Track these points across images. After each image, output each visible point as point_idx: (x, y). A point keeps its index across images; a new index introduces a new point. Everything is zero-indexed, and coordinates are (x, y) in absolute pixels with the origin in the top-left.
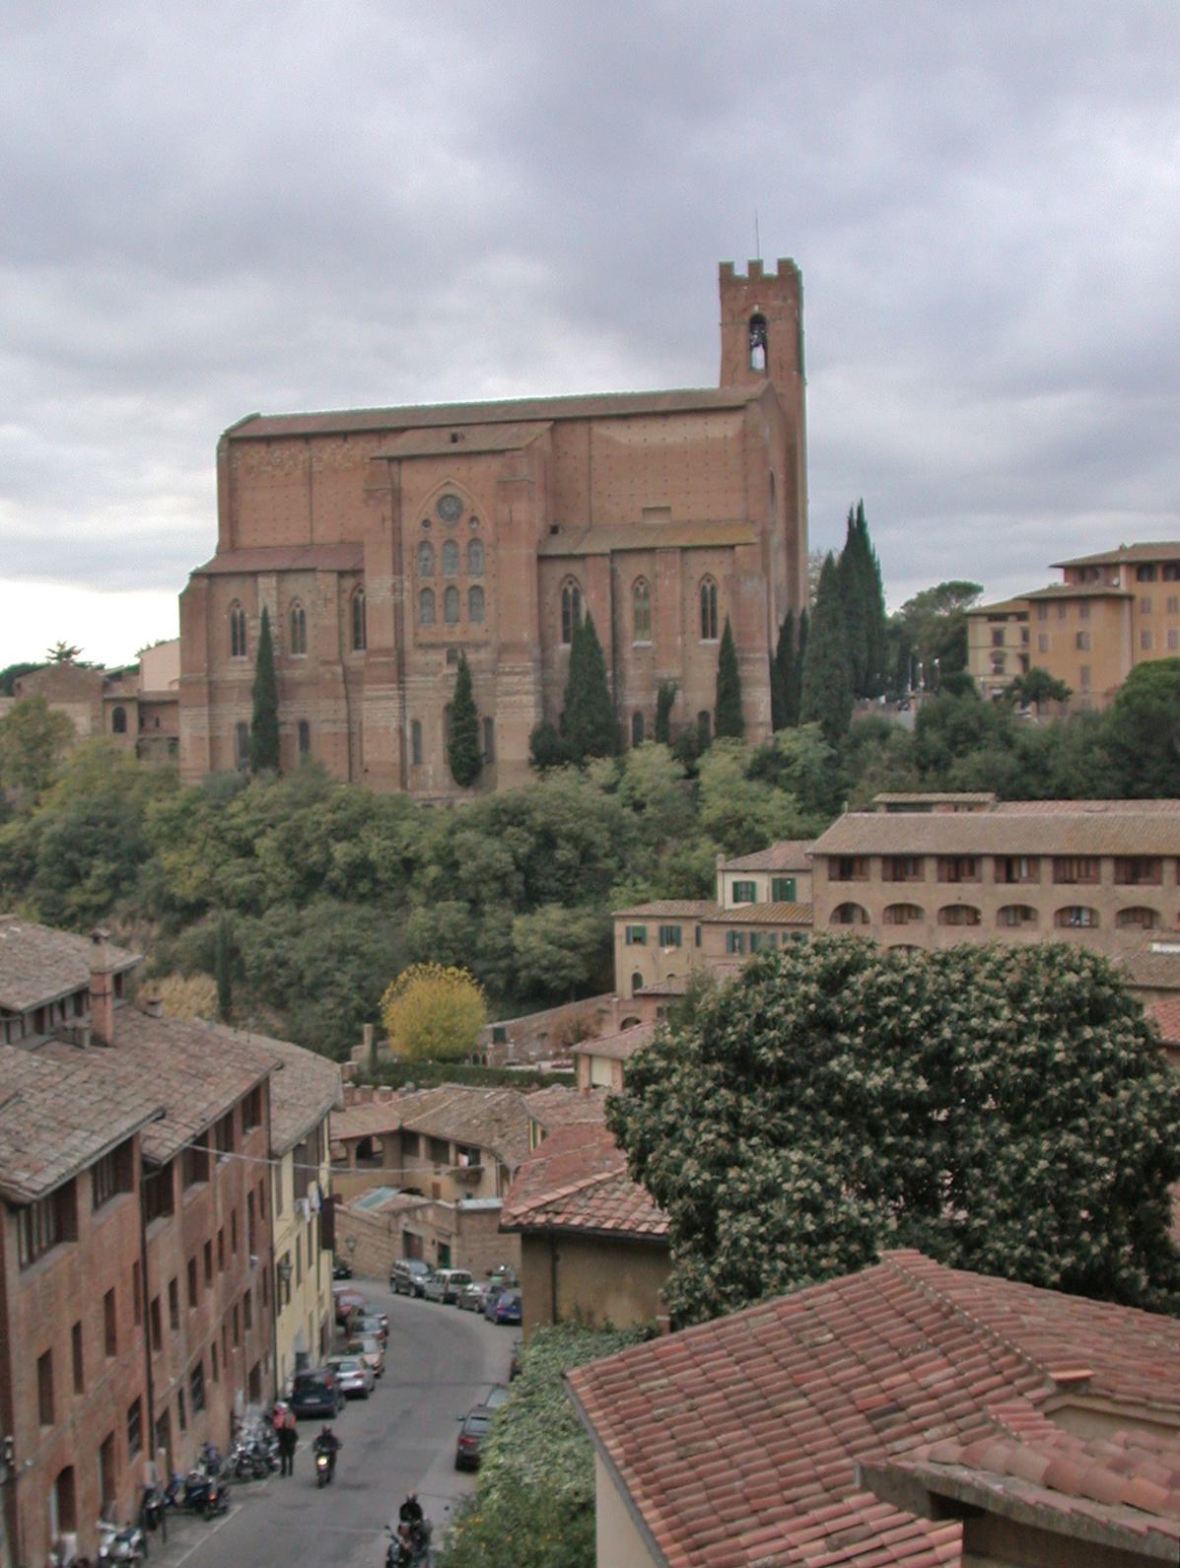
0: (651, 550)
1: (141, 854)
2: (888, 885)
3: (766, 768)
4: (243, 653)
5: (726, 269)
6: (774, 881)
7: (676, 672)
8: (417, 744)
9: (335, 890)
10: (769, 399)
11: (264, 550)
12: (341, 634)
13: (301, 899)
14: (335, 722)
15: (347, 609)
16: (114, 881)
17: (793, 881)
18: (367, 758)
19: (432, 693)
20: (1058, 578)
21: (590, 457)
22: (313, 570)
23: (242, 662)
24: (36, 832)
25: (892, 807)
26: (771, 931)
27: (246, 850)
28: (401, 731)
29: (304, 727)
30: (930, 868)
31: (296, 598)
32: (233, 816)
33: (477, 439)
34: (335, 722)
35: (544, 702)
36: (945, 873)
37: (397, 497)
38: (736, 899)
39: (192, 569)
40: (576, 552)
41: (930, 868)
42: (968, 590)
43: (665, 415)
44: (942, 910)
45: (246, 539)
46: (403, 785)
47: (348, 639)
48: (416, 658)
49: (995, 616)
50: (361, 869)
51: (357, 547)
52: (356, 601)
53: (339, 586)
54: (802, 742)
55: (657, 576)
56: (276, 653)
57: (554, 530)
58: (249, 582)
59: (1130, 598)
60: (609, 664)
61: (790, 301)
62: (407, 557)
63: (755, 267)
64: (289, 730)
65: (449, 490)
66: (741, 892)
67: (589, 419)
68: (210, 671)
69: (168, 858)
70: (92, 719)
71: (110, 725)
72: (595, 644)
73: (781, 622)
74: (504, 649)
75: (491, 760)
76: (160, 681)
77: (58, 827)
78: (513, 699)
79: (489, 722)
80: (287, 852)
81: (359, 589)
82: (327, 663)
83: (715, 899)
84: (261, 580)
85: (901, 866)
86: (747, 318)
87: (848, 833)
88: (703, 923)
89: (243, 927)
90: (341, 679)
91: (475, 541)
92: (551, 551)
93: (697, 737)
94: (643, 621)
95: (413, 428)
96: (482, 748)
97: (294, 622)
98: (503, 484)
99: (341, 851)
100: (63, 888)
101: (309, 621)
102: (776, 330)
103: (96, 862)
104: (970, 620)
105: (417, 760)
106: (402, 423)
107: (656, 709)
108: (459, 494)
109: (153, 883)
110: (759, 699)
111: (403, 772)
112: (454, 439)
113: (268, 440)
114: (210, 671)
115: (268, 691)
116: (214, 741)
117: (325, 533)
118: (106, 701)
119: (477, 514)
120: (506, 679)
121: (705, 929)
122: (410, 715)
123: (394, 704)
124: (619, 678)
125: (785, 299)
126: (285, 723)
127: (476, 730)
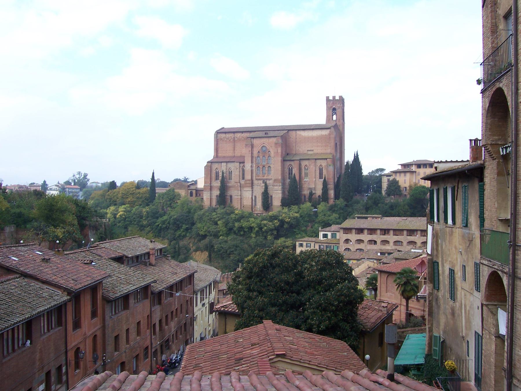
0: (309, 159)
1: (193, 224)
2: (356, 235)
3: (332, 209)
4: (218, 180)
5: (328, 98)
6: (332, 233)
7: (313, 186)
8: (255, 201)
9: (235, 233)
10: (336, 127)
11: (224, 157)
12: (240, 176)
13: (227, 235)
14: (238, 196)
15: (241, 170)
16: (187, 230)
17: (336, 234)
18: (244, 204)
19: (259, 190)
20: (400, 167)
21: (296, 138)
22: (234, 162)
23: (218, 182)
24: (171, 217)
25: (358, 218)
26: (330, 245)
27: (216, 224)
28: (252, 198)
29: (231, 196)
30: (366, 231)
31: (230, 168)
32: (214, 215)
33: (271, 134)
34: (238, 196)
35: (283, 193)
36: (369, 232)
37: (252, 146)
38: (323, 238)
39: (208, 161)
40: (292, 159)
41: (366, 231)
42: (382, 170)
43: (313, 129)
44: (368, 241)
45: (220, 155)
46: (252, 210)
47: (241, 177)
48: (255, 182)
49: (388, 175)
50: (241, 228)
51: (244, 157)
52: (243, 169)
53: (239, 166)
54: (341, 202)
55: (310, 165)
56: (225, 180)
57: (288, 154)
58: (220, 164)
59: (415, 172)
60: (299, 185)
61: (341, 105)
62: (254, 159)
63: (334, 97)
64: (229, 197)
65: (264, 145)
66: (325, 236)
67: (296, 130)
68: (211, 184)
69: (199, 225)
70: (186, 193)
71: (189, 195)
72: (296, 180)
73: (338, 176)
74: (275, 180)
75: (272, 205)
76: (201, 185)
77: (175, 217)
78: (277, 191)
79: (271, 196)
80: (226, 224)
81: (244, 166)
82: (236, 182)
83: (319, 237)
84: (222, 164)
85: (360, 231)
86: (332, 109)
87: (347, 224)
88: (315, 243)
89: (215, 241)
90: (239, 186)
91: (269, 156)
92: (285, 159)
93: (318, 201)
94: (306, 175)
95: (258, 131)
96: (270, 202)
97: (230, 173)
98: (276, 144)
99: (236, 224)
100: (176, 231)
101: (233, 173)
102: (339, 111)
103: (183, 225)
104: (382, 176)
105: (255, 205)
106: (254, 130)
107: (309, 195)
108: (266, 146)
109: (196, 230)
110: (332, 193)
111: (252, 207)
112: (266, 134)
113: (225, 133)
114: (211, 184)
115: (224, 188)
116: (211, 199)
117: (238, 153)
118: (188, 189)
119: (270, 150)
120: (275, 187)
121: (316, 244)
122: (254, 195)
123: (251, 192)
124: (301, 187)
125: (340, 104)
126: (227, 196)
127: (269, 198)
